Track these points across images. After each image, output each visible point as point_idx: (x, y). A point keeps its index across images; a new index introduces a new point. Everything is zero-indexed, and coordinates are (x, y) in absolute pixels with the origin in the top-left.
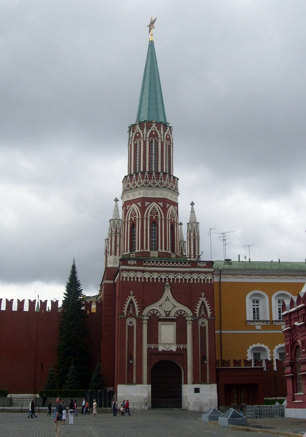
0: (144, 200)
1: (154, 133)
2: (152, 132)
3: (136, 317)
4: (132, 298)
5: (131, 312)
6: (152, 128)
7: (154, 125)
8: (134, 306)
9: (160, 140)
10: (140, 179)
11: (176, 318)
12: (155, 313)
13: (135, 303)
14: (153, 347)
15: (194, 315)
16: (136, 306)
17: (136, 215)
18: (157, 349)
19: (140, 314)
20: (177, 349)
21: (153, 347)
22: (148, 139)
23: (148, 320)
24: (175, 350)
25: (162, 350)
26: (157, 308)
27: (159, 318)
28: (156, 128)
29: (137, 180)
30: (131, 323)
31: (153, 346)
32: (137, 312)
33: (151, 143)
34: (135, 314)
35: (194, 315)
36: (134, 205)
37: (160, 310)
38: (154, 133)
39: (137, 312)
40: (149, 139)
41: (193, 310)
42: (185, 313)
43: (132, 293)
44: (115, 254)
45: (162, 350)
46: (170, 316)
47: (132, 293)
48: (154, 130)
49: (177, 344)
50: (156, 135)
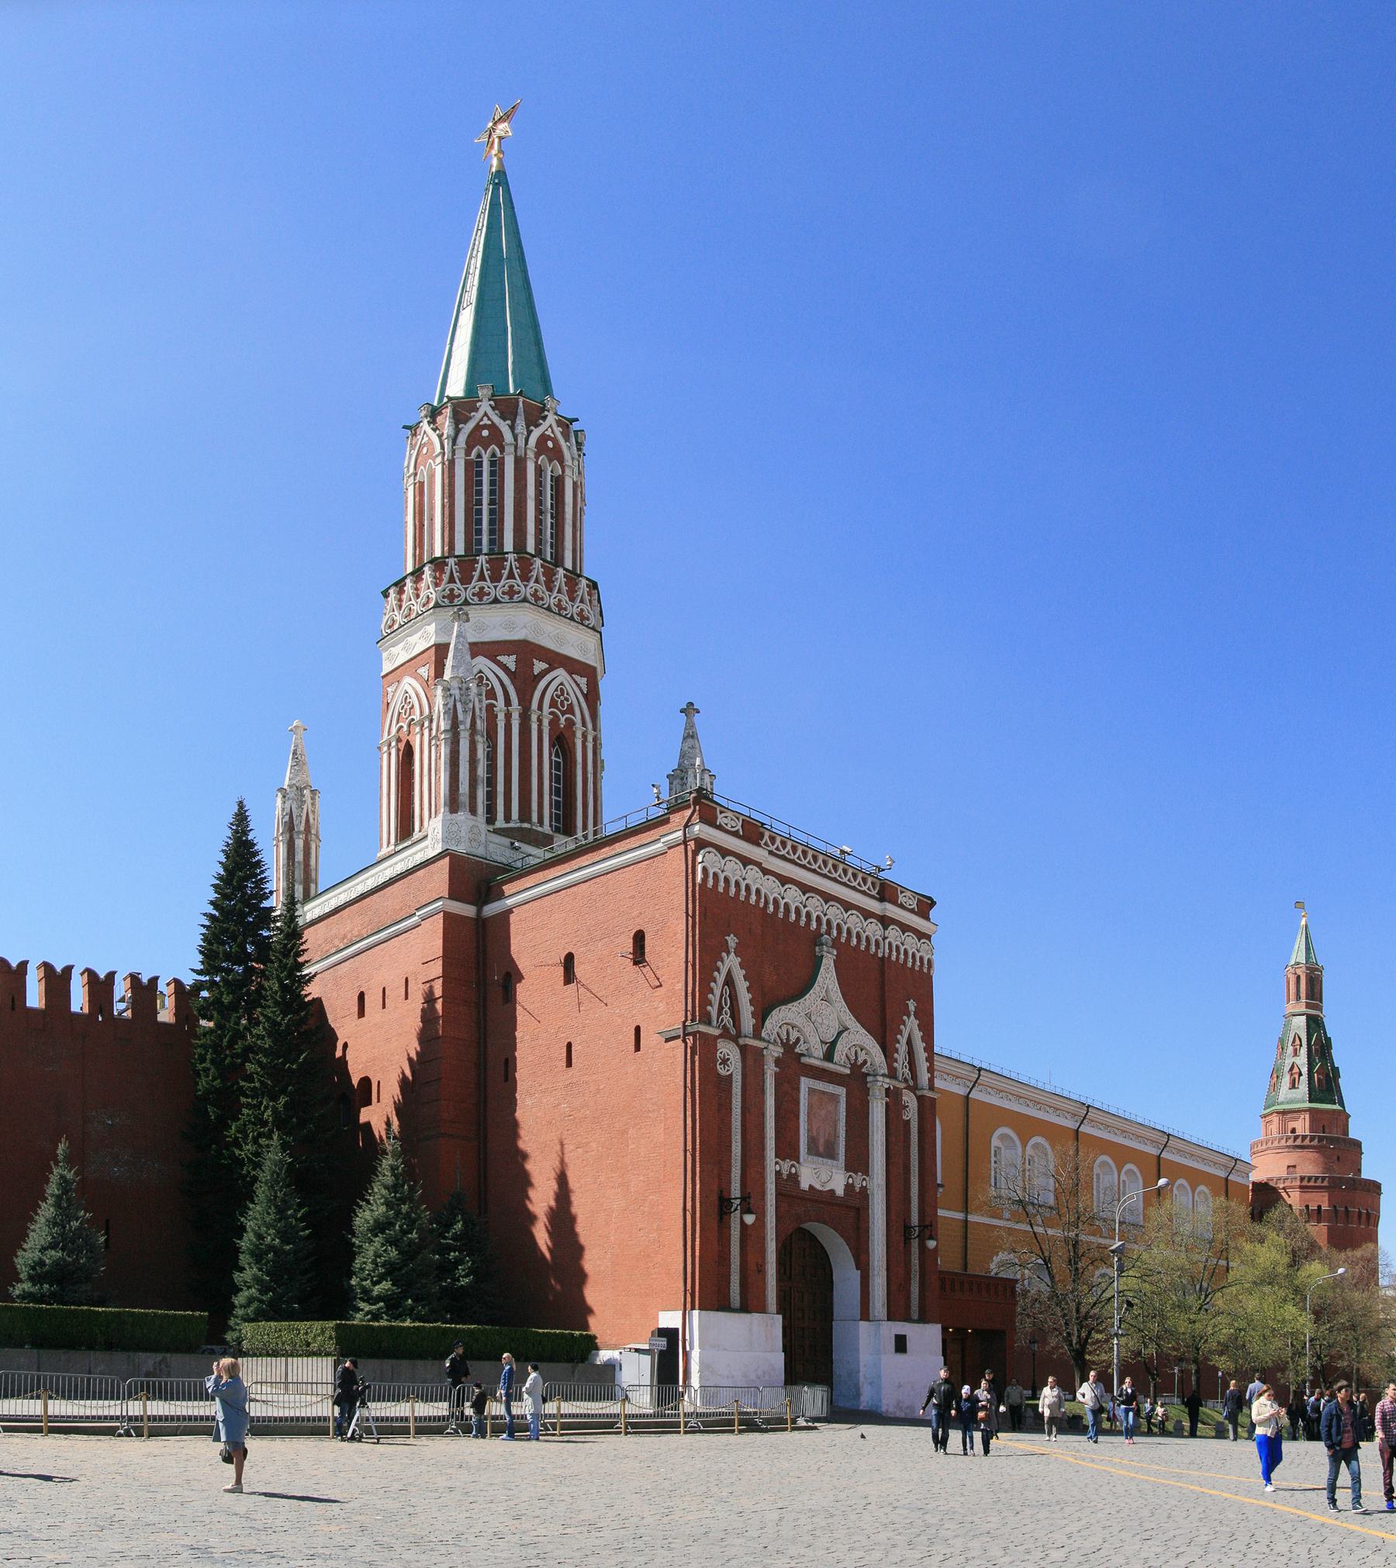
0: (526, 650)
1: (550, 444)
2: (543, 438)
3: (741, 1041)
4: (731, 962)
5: (727, 1018)
6: (545, 425)
7: (551, 419)
8: (734, 998)
9: (568, 472)
10: (511, 576)
11: (848, 1071)
12: (792, 1040)
13: (742, 985)
14: (785, 1173)
15: (892, 1074)
16: (744, 997)
17: (491, 694)
18: (794, 1178)
19: (757, 1034)
20: (849, 1187)
21: (785, 1173)
22: (531, 455)
23: (778, 1062)
24: (840, 1192)
25: (811, 1187)
26: (799, 1021)
27: (804, 1060)
28: (558, 430)
29: (496, 578)
30: (725, 1062)
31: (786, 1166)
32: (748, 1022)
33: (539, 471)
34: (739, 1035)
35: (892, 1074)
36: (482, 663)
37: (808, 1029)
38: (550, 444)
39: (748, 1022)
40: (537, 458)
41: (888, 1049)
42: (865, 1062)
43: (732, 941)
44: (473, 811)
45: (811, 1187)
46: (835, 1059)
47: (732, 941)
48: (549, 432)
49: (848, 1168)
50: (557, 454)
